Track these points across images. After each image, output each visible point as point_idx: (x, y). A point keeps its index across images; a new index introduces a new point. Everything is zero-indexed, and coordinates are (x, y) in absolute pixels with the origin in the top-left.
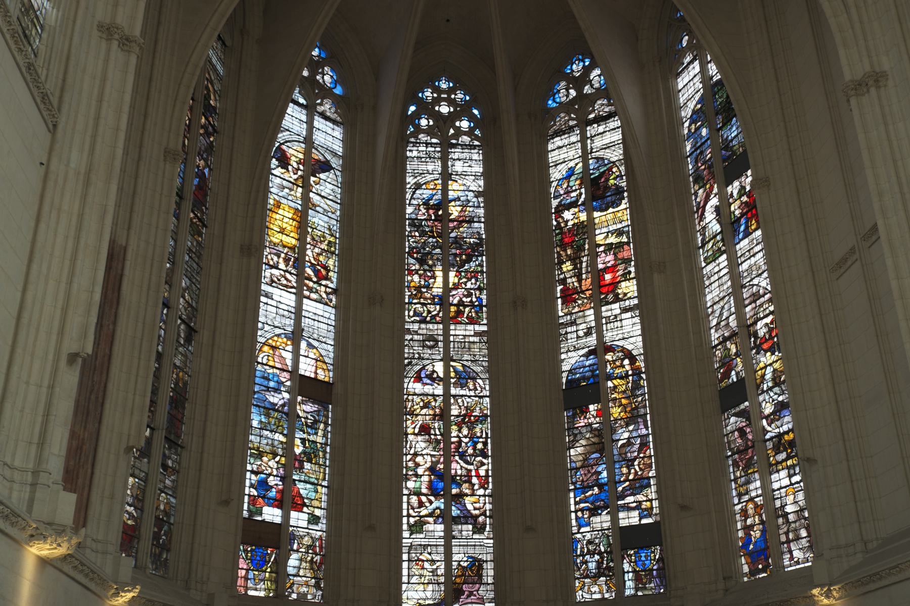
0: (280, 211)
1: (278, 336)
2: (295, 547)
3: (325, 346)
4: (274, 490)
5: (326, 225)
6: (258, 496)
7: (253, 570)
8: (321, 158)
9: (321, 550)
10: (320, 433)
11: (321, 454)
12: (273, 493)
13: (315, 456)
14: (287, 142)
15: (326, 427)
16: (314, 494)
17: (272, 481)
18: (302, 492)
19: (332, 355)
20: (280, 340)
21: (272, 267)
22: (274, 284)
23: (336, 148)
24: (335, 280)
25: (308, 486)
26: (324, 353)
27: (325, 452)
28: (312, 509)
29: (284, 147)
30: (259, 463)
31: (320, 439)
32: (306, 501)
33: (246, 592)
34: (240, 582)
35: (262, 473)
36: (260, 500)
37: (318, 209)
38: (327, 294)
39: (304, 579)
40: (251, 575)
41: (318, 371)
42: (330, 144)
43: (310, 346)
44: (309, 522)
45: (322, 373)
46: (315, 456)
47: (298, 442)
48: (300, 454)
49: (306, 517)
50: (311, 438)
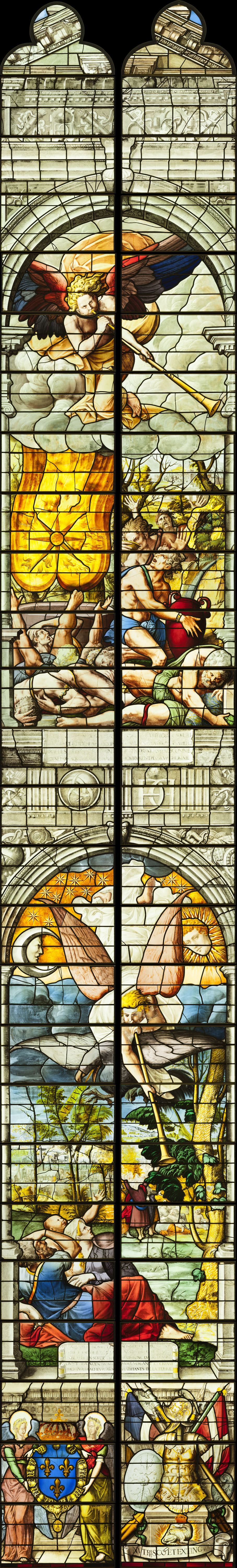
0: (49, 482)
1: (67, 869)
2: (145, 1432)
3: (207, 853)
4: (86, 1296)
5: (188, 466)
6: (44, 1321)
7: (42, 1503)
8: (162, 237)
9: (223, 1430)
10: (204, 1113)
11: (208, 1171)
12: (84, 1305)
13: (191, 1182)
14: (50, 239)
15: (220, 1096)
16: (194, 1287)
17: (78, 1275)
18: (155, 1287)
19: (229, 874)
20: (72, 879)
21: (33, 670)
22: (46, 720)
23: (207, 171)
24: (227, 635)
25: (176, 1268)
26: (200, 876)
27: (220, 1164)
28: (189, 1327)
29: (45, 261)
30: (36, 1235)
31: (203, 1132)
32: (169, 1308)
33: (31, 1557)
34: (10, 1535)
35: (47, 1258)
36: (50, 1328)
37: (157, 422)
38: (202, 690)
39: (177, 1508)
40: (40, 1515)
41: (188, 937)
42: (185, 171)
43: (158, 869)
44: (182, 1364)
45: (201, 939)
46: (191, 1182)
47: (132, 1154)
48: (143, 1187)
49: (171, 1351)
50: (176, 1135)
